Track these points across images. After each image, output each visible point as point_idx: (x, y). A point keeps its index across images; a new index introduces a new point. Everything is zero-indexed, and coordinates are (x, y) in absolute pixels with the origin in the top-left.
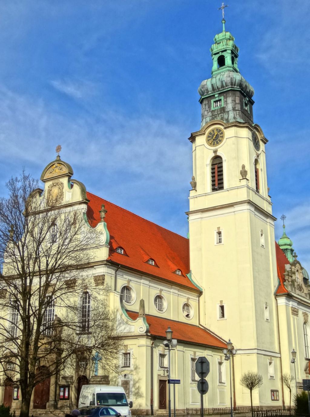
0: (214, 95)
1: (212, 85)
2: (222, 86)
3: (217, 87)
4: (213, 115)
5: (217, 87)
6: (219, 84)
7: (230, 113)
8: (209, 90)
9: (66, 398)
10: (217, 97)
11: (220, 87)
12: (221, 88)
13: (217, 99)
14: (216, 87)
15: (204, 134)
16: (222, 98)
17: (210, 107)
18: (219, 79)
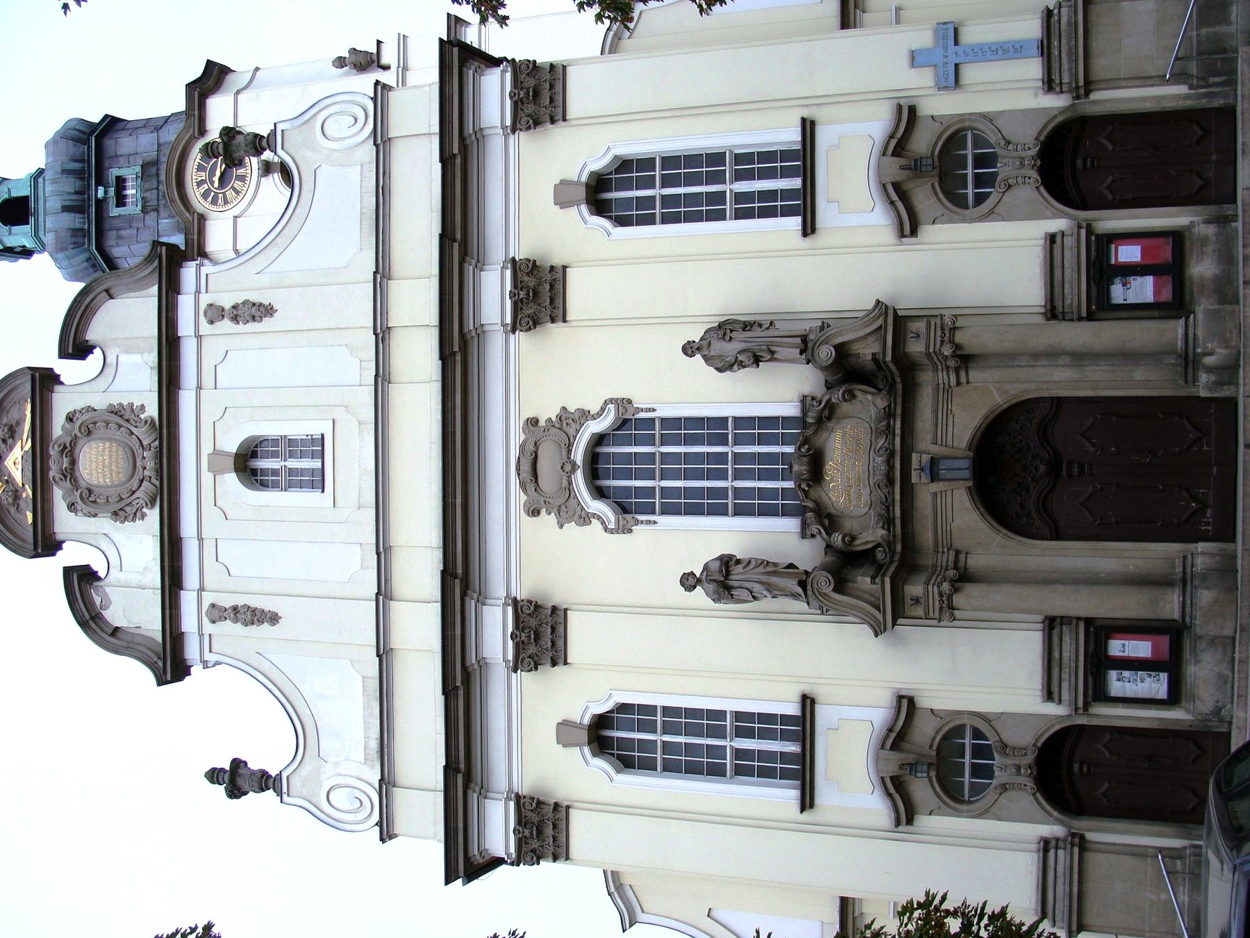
0: (100, 204)
1: (66, 209)
2: (80, 174)
3: (76, 193)
4: (157, 210)
5: (76, 193)
6: (70, 185)
7: (162, 141)
8: (78, 226)
9: (1165, 654)
10: (106, 192)
11: (78, 183)
12: (82, 179)
13: (112, 191)
14: (75, 197)
15: (202, 219)
16: (114, 172)
17: (130, 220)
18: (54, 181)
